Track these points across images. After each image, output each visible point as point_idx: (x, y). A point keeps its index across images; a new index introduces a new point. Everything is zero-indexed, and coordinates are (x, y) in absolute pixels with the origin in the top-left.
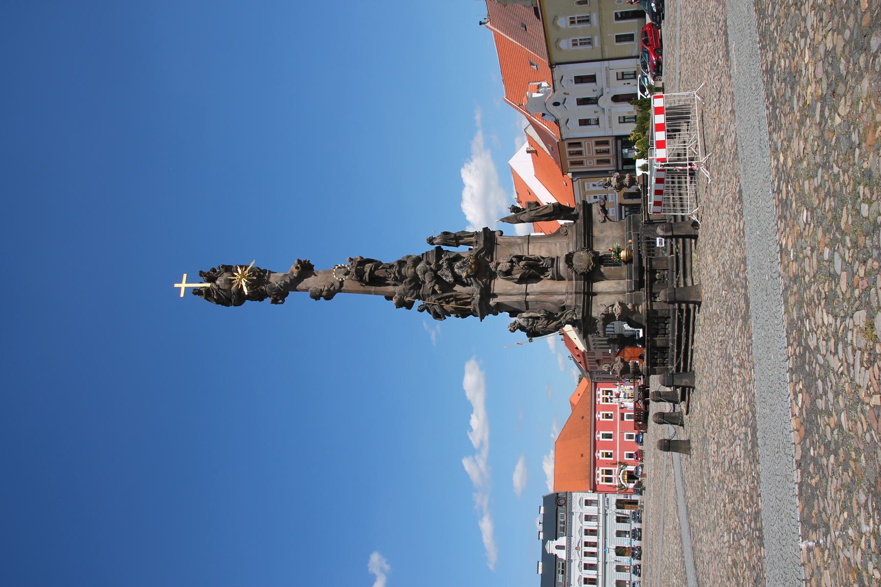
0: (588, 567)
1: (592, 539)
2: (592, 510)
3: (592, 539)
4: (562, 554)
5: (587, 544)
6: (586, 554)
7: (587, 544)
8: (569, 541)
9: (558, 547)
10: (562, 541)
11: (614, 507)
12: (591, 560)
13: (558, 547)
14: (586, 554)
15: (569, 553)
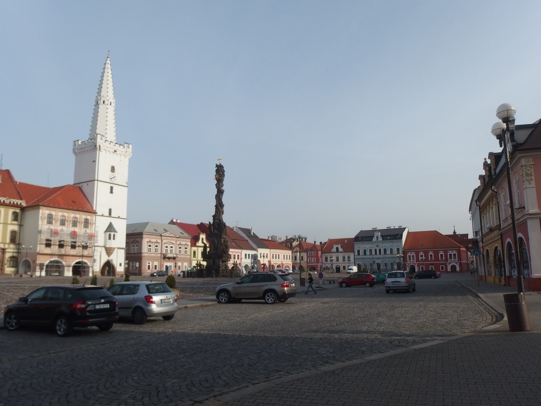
0: (371, 251)
1: (382, 252)
2: (395, 251)
3: (382, 252)
4: (374, 239)
5: (380, 250)
6: (376, 250)
7: (380, 250)
8: (380, 242)
9: (377, 237)
10: (380, 239)
11: (397, 261)
12: (374, 253)
13: (377, 237)
14: (376, 250)
15: (375, 242)
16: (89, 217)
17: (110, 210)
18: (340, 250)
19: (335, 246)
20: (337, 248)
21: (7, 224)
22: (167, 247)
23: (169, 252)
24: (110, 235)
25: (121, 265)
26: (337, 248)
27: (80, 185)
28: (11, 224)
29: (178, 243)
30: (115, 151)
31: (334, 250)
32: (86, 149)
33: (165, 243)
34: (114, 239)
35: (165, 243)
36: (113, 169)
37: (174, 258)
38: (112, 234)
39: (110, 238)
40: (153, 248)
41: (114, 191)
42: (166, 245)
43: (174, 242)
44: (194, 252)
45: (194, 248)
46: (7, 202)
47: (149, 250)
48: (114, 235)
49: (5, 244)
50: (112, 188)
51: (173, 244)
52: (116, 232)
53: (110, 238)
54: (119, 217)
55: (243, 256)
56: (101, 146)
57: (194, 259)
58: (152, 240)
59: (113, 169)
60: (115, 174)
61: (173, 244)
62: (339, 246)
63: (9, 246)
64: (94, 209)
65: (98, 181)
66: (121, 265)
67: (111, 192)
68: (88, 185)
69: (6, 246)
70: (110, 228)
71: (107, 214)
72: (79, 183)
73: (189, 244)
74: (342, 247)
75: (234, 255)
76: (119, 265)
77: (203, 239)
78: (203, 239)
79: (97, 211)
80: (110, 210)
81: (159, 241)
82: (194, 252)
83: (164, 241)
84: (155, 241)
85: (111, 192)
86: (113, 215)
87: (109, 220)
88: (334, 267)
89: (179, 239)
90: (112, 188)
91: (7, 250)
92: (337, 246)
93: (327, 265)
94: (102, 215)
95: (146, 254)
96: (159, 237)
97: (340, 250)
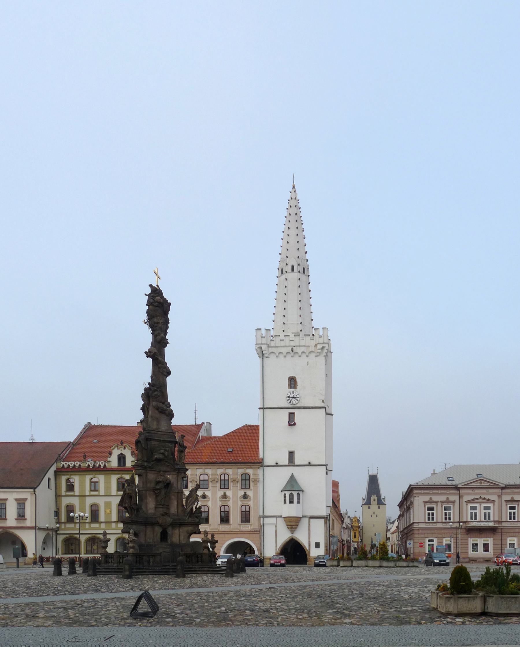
16: (250, 471)
17: (291, 454)
23: (480, 516)
25: (317, 545)
34: (298, 502)
36: (293, 382)
37: (492, 530)
38: (295, 494)
39: (285, 503)
40: (439, 513)
41: (297, 420)
42: (470, 505)
47: (431, 517)
48: (298, 495)
50: (292, 415)
51: (493, 502)
54: (310, 464)
58: (435, 498)
59: (293, 382)
60: (298, 391)
61: (493, 502)
64: (261, 456)
66: (317, 545)
76: (313, 545)
80: (291, 454)
81: (455, 498)
84: (444, 498)
86: (297, 462)
87: (289, 471)
94: (277, 465)
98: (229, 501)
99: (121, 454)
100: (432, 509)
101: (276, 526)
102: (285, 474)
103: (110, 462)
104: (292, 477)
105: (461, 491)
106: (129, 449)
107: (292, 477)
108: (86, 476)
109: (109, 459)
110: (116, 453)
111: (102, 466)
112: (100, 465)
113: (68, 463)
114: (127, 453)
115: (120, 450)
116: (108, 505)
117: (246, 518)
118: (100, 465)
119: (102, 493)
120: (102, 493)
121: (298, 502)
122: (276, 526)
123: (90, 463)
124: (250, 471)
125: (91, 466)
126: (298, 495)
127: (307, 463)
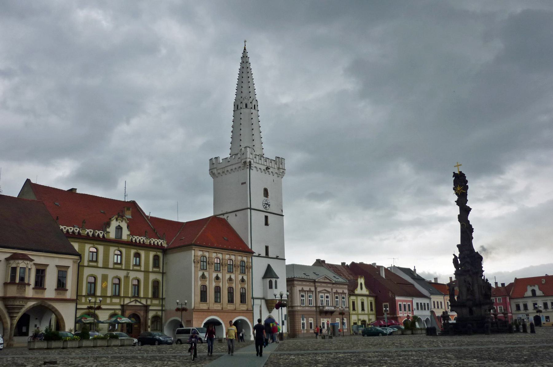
17: (267, 248)
18: (538, 293)
19: (529, 289)
20: (533, 292)
21: (149, 272)
22: (322, 297)
24: (271, 282)
26: (533, 292)
27: (225, 217)
28: (153, 272)
29: (334, 290)
30: (268, 168)
31: (529, 293)
32: (229, 169)
33: (320, 292)
35: (320, 292)
39: (271, 287)
41: (269, 222)
43: (329, 290)
44: (353, 303)
45: (353, 298)
46: (147, 242)
49: (147, 299)
50: (266, 217)
51: (328, 292)
52: (278, 278)
53: (271, 287)
55: (415, 306)
56: (252, 162)
57: (354, 312)
60: (270, 200)
61: (328, 292)
62: (536, 288)
63: (151, 302)
64: (250, 248)
65: (251, 209)
67: (267, 224)
68: (236, 215)
69: (149, 302)
70: (269, 273)
71: (264, 254)
72: (223, 214)
73: (346, 291)
74: (540, 289)
75: (405, 305)
77: (361, 284)
78: (361, 284)
79: (253, 250)
81: (313, 289)
82: (353, 303)
83: (319, 289)
85: (267, 224)
86: (270, 255)
87: (267, 261)
88: (531, 318)
89: (334, 286)
90: (266, 217)
91: (151, 308)
92: (533, 288)
93: (520, 316)
95: (299, 308)
96: (312, 284)
97: (538, 293)
98: (220, 282)
99: (119, 226)
100: (302, 296)
101: (261, 307)
102: (265, 262)
103: (109, 232)
104: (269, 266)
105: (317, 284)
106: (126, 222)
107: (269, 266)
108: (86, 245)
109: (108, 230)
110: (114, 224)
111: (101, 235)
112: (98, 235)
113: (67, 228)
114: (124, 225)
115: (118, 222)
116: (105, 278)
117: (243, 299)
118: (98, 235)
119: (100, 264)
120: (100, 264)
121: (276, 288)
122: (261, 307)
123: (90, 232)
124: (245, 259)
125: (91, 234)
126: (276, 282)
127: (275, 256)
